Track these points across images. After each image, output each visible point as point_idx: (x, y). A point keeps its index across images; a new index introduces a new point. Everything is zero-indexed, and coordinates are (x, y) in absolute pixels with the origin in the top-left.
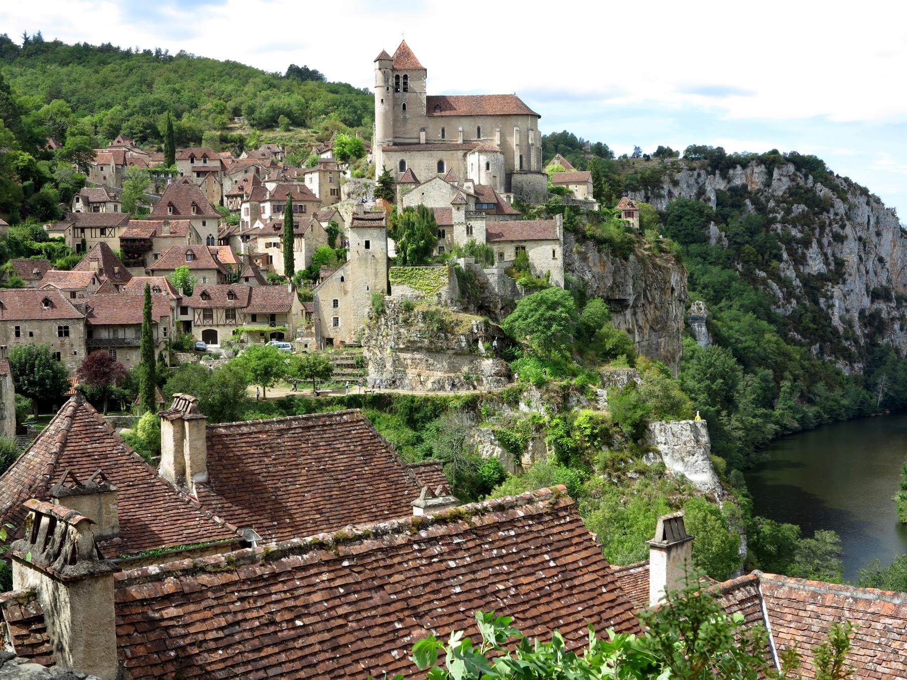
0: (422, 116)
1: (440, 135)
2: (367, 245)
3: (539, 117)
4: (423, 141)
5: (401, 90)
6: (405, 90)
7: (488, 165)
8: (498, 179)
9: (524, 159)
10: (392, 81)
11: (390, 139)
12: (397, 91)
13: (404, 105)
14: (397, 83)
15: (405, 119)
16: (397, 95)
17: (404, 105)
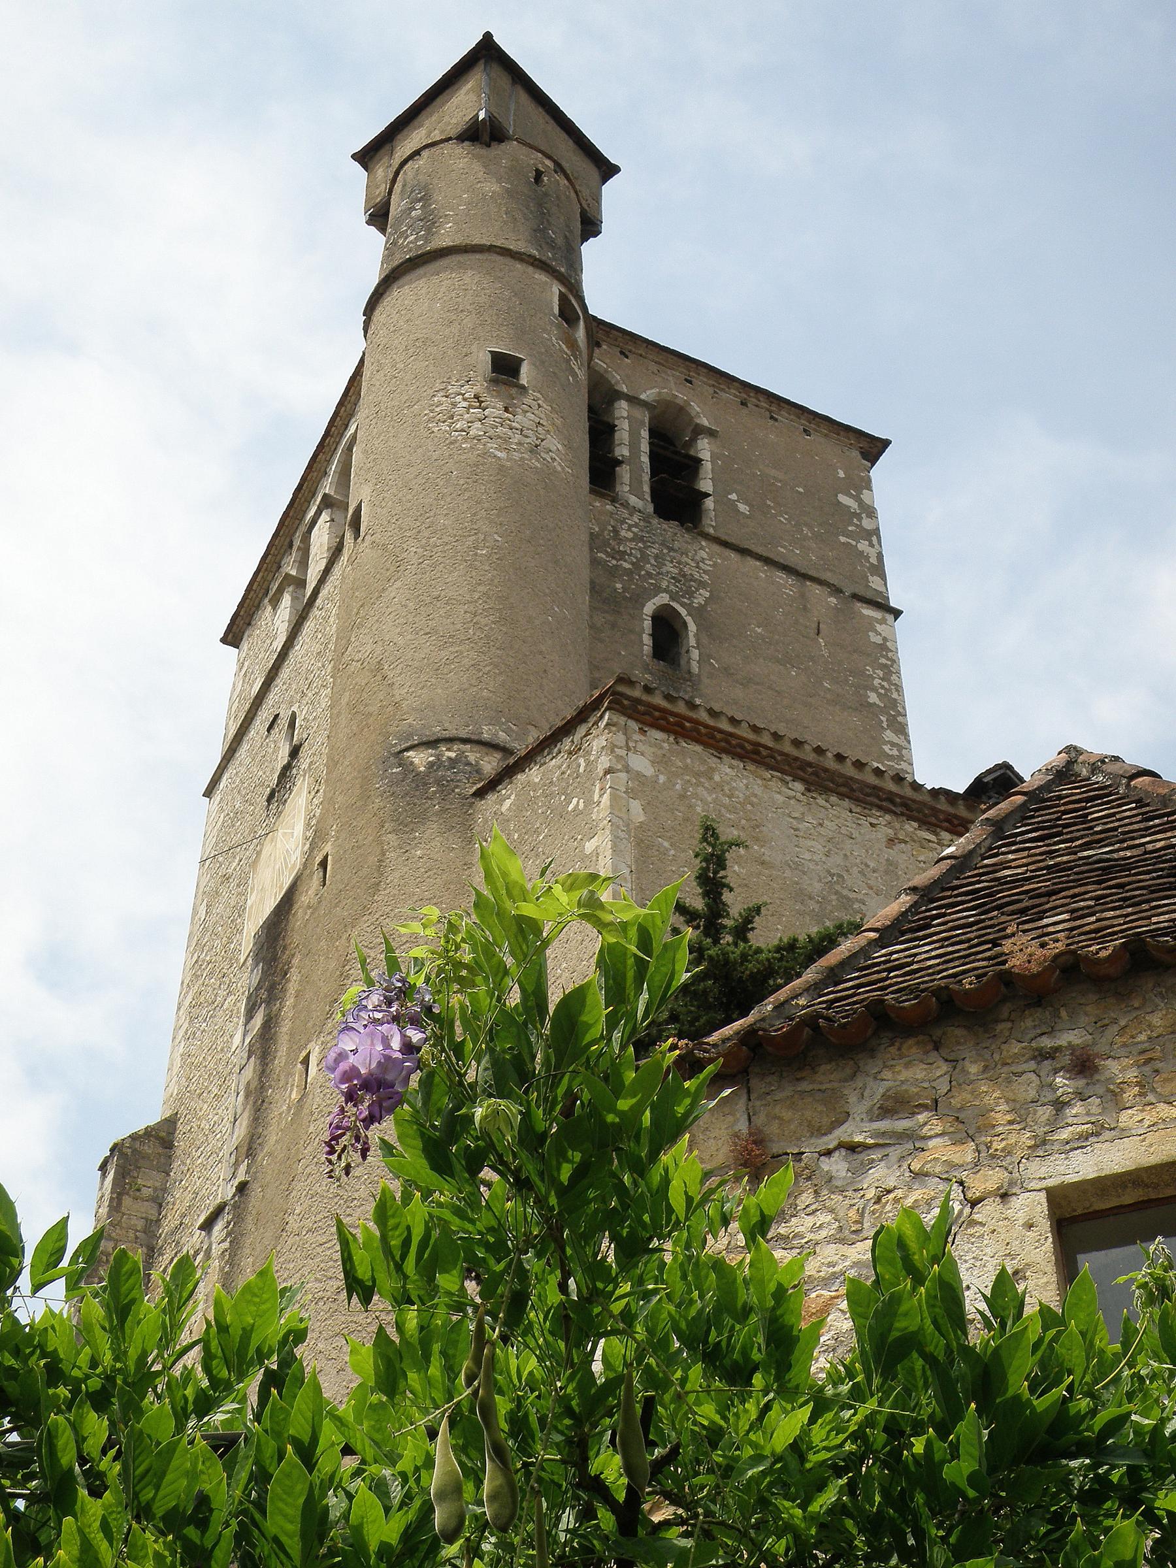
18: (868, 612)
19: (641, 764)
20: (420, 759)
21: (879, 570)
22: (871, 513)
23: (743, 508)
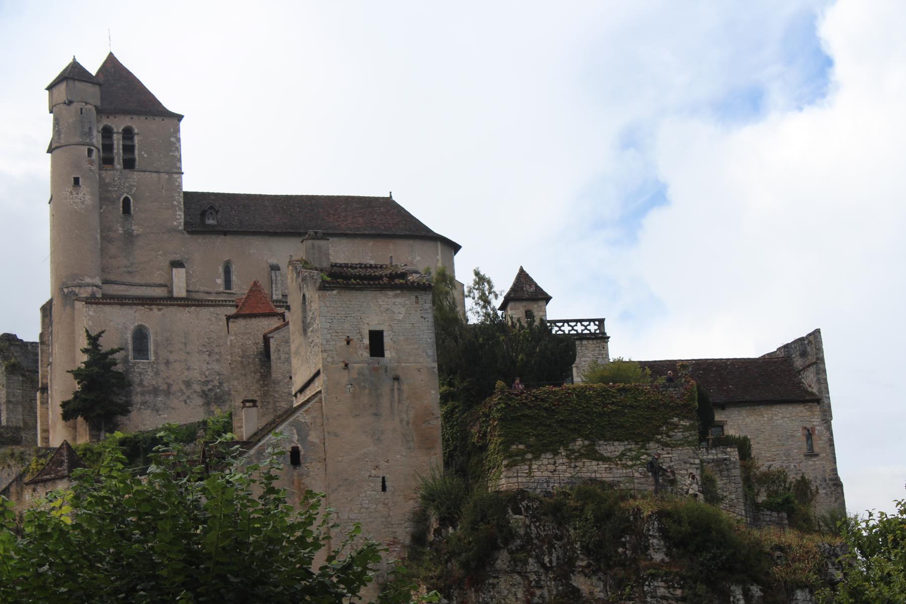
0: (174, 230)
1: (220, 281)
2: (376, 342)
3: (456, 248)
4: (179, 290)
6: (129, 164)
10: (97, 139)
11: (97, 281)
12: (107, 161)
13: (126, 202)
14: (108, 148)
15: (129, 238)
16: (108, 175)
17: (126, 202)
18: (176, 176)
19: (91, 313)
20: (66, 290)
21: (180, 160)
22: (179, 140)
23: (146, 156)
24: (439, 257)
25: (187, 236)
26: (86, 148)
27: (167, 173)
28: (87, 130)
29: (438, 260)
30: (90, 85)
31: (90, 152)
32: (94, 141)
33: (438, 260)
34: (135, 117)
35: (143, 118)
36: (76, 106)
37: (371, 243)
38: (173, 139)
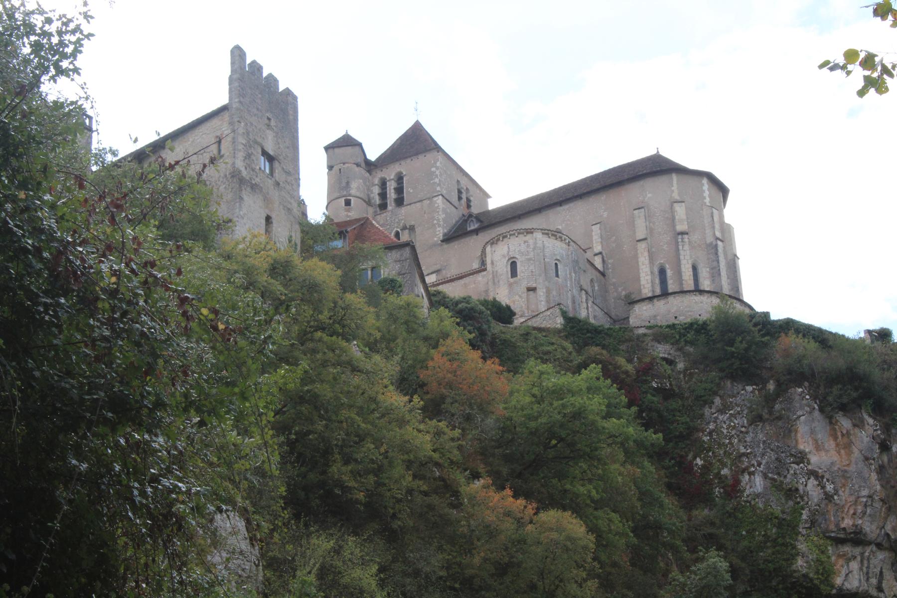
5: (391, 206)
6: (400, 202)
7: (513, 265)
8: (541, 293)
9: (669, 273)
14: (383, 195)
24: (675, 188)
25: (445, 246)
26: (342, 201)
27: (429, 199)
28: (344, 184)
29: (673, 191)
30: (350, 148)
31: (348, 203)
32: (353, 192)
33: (673, 191)
34: (403, 162)
35: (409, 161)
36: (336, 168)
37: (603, 197)
38: (433, 169)
